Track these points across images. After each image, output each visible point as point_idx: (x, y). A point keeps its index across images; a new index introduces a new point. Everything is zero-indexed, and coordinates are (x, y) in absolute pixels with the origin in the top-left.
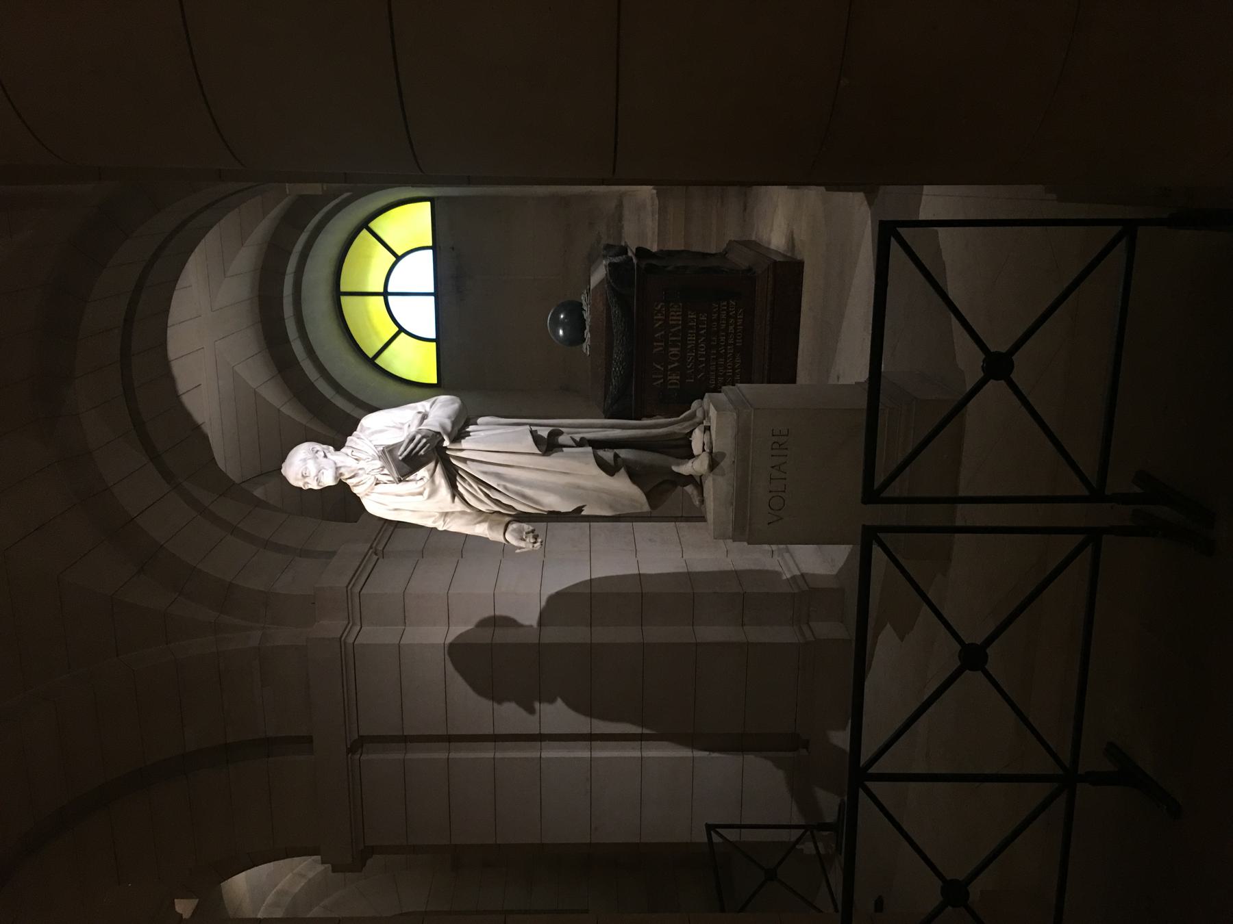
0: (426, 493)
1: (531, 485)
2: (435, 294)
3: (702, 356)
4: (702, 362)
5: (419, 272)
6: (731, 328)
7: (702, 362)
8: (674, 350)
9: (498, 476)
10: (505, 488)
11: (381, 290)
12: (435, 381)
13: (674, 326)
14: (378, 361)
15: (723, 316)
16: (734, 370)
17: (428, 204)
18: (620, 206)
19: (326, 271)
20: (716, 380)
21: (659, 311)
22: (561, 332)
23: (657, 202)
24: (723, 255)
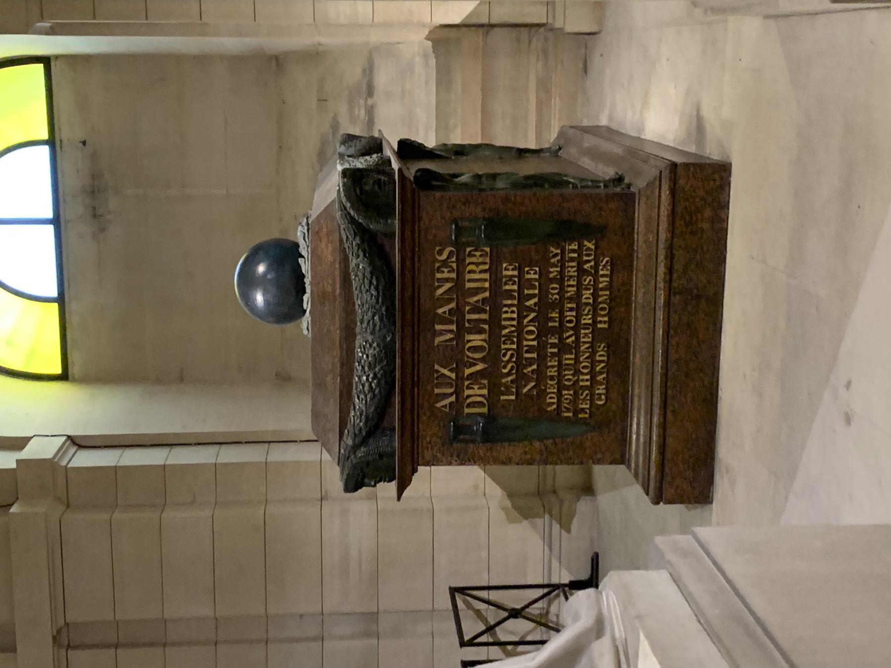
3: (530, 349)
4: (530, 362)
6: (587, 294)
7: (530, 362)
8: (476, 340)
12: (58, 370)
13: (477, 291)
15: (573, 272)
16: (593, 374)
18: (369, 71)
21: (445, 263)
23: (433, 62)
24: (555, 152)
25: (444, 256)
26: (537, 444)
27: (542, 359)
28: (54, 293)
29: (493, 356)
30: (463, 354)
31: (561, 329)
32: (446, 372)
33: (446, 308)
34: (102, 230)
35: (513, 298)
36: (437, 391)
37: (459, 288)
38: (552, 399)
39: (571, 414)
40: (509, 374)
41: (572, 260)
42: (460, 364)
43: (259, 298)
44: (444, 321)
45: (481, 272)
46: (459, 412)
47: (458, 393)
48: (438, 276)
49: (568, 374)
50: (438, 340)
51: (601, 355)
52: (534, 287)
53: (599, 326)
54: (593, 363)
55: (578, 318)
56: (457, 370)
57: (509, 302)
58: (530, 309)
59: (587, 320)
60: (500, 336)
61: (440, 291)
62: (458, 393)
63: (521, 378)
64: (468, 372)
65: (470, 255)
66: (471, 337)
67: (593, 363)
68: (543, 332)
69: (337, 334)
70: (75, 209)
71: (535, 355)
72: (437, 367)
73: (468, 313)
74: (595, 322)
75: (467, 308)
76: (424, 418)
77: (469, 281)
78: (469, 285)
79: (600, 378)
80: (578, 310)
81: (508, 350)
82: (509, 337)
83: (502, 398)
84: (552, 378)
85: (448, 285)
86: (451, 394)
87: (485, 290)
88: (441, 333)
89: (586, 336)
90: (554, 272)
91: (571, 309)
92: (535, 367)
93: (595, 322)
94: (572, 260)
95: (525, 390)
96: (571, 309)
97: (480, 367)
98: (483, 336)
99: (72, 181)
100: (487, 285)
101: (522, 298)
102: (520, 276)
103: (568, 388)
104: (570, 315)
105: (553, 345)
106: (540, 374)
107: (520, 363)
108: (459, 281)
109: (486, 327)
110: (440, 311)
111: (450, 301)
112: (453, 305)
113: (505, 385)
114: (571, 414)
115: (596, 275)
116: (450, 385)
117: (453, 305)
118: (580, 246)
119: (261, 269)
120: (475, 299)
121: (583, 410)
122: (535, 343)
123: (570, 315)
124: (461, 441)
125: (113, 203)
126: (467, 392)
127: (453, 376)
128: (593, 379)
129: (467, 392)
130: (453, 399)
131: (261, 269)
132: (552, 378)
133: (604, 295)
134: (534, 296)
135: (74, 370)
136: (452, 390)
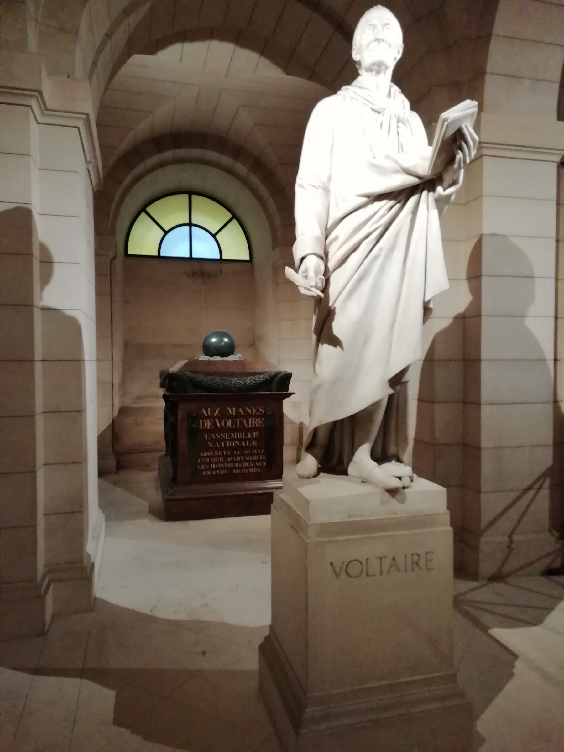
2: (191, 258)
3: (225, 444)
5: (205, 249)
6: (246, 464)
7: (220, 445)
8: (229, 423)
9: (392, 249)
10: (376, 258)
11: (188, 222)
12: (130, 252)
14: (143, 215)
15: (256, 458)
16: (215, 469)
17: (247, 258)
19: (209, 186)
20: (207, 457)
21: (258, 411)
22: (214, 340)
25: (261, 410)
27: (221, 449)
29: (223, 430)
31: (232, 455)
32: (217, 412)
33: (241, 412)
35: (245, 436)
36: (209, 409)
37: (248, 416)
39: (199, 461)
40: (216, 437)
41: (259, 458)
42: (220, 418)
44: (237, 410)
45: (255, 424)
47: (208, 417)
48: (254, 408)
50: (229, 409)
51: (223, 472)
52: (249, 444)
53: (234, 470)
54: (220, 469)
55: (238, 462)
56: (217, 417)
58: (241, 443)
59: (237, 465)
61: (248, 409)
62: (208, 417)
63: (214, 441)
64: (217, 421)
65: (261, 420)
66: (230, 421)
67: (220, 469)
68: (232, 449)
69: (231, 370)
70: (196, 266)
72: (219, 409)
73: (240, 420)
74: (236, 468)
77: (252, 420)
78: (250, 419)
79: (214, 473)
80: (241, 462)
81: (225, 435)
82: (230, 436)
83: (206, 435)
84: (214, 453)
85: (250, 412)
87: (248, 425)
89: (230, 465)
90: (255, 451)
91: (241, 459)
93: (236, 468)
94: (259, 458)
95: (209, 443)
96: (241, 459)
97: (219, 425)
98: (230, 426)
99: (207, 267)
100: (250, 426)
101: (245, 440)
102: (254, 439)
103: (210, 460)
104: (239, 459)
105: (227, 453)
106: (215, 449)
107: (220, 441)
108: (251, 416)
110: (240, 409)
112: (242, 414)
113: (212, 435)
114: (199, 461)
115: (253, 467)
117: (242, 414)
118: (264, 461)
119: (226, 340)
121: (201, 467)
122: (228, 446)
123: (239, 459)
126: (208, 421)
128: (213, 469)
129: (208, 421)
130: (206, 415)
131: (226, 340)
132: (214, 453)
133: (246, 471)
134: (246, 443)
136: (209, 415)
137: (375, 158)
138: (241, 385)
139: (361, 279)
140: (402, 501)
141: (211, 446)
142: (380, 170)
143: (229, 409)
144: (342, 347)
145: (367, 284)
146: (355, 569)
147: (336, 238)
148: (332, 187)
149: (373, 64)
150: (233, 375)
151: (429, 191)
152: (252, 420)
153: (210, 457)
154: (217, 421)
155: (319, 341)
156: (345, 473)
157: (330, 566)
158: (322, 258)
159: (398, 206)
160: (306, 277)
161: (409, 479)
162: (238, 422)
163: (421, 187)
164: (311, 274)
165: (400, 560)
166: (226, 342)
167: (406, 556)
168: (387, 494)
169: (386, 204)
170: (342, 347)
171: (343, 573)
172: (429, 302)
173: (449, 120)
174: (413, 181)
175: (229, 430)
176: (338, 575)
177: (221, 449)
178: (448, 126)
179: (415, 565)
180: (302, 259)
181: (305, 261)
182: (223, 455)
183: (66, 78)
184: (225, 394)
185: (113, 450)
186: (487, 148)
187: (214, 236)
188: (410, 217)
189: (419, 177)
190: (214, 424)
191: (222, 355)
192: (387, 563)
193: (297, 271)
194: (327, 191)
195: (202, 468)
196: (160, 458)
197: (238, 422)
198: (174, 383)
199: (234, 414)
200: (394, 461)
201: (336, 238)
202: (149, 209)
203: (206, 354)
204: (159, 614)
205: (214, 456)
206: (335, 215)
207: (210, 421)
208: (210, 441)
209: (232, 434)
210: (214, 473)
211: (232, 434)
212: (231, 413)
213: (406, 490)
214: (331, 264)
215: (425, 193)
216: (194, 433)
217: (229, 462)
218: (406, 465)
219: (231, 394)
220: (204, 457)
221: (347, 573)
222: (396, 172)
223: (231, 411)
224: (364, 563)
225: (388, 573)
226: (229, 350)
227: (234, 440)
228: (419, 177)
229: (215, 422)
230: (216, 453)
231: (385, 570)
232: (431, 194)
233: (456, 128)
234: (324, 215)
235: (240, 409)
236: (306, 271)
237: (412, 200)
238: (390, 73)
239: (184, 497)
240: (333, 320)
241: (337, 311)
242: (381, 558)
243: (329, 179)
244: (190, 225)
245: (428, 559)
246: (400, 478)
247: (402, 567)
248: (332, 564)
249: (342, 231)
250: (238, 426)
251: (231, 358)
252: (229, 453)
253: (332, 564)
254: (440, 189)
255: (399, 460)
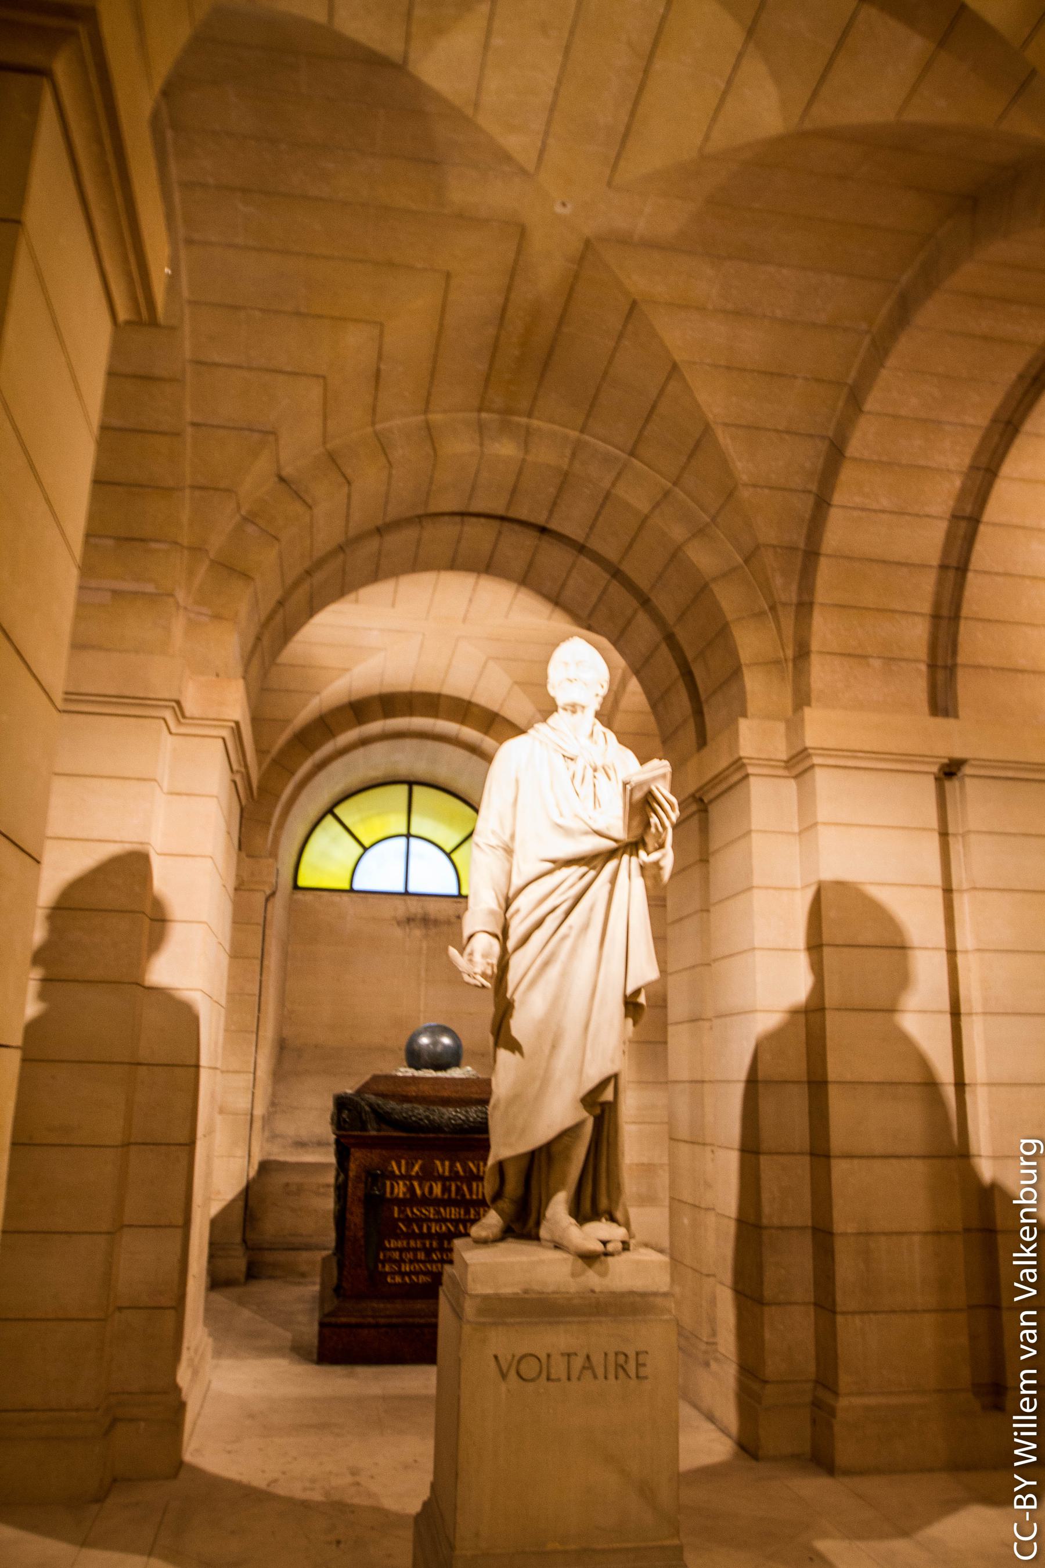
0: (560, 821)
1: (564, 974)
3: (429, 1228)
7: (420, 1228)
8: (437, 1190)
9: (586, 927)
10: (565, 937)
11: (404, 831)
12: (301, 883)
19: (442, 773)
20: (396, 1249)
26: (360, 1234)
27: (422, 1236)
28: (357, 886)
29: (426, 1201)
30: (428, 1180)
32: (416, 1168)
34: (399, 923)
36: (403, 1162)
38: (393, 1244)
40: (413, 1213)
43: (424, 1040)
44: (452, 1167)
46: (388, 1178)
47: (402, 1177)
49: (410, 1255)
50: (438, 1163)
51: (422, 1279)
54: (417, 1273)
56: (417, 1177)
57: (462, 1212)
58: (456, 1227)
60: (439, 1206)
61: (471, 1165)
62: (402, 1177)
63: (408, 1221)
64: (416, 1184)
66: (440, 1185)
67: (417, 1273)
69: (445, 1094)
70: (414, 907)
71: (425, 1230)
72: (420, 1162)
73: (457, 1186)
75: (459, 1184)
76: (384, 1152)
77: (478, 1186)
79: (407, 1279)
82: (438, 1213)
83: (396, 1209)
84: (408, 1244)
85: (475, 1170)
86: (400, 1171)
88: (443, 1165)
92: (417, 1231)
97: (418, 1192)
99: (433, 908)
100: (474, 1197)
103: (401, 1256)
105: (431, 1244)
107: (419, 1221)
109: (446, 1196)
110: (458, 1165)
111: (464, 1171)
112: (462, 1173)
113: (405, 1211)
116: (407, 1170)
119: (446, 1040)
120: (465, 1188)
121: (384, 1266)
122: (433, 1231)
124: (367, 1179)
125: (418, 933)
127: (413, 1173)
129: (401, 1183)
130: (397, 1172)
132: (408, 1244)
135: (299, 896)
137: (561, 815)
138: (460, 1122)
139: (546, 964)
140: (603, 1274)
141: (404, 1229)
142: (567, 832)
143: (438, 1163)
144: (521, 1053)
145: (553, 972)
146: (529, 1368)
147: (517, 911)
148: (517, 846)
149: (568, 705)
150: (446, 1102)
151: (631, 855)
152: (478, 1186)
153: (401, 1250)
154: (416, 1184)
155: (496, 1045)
156: (537, 1238)
157: (493, 1359)
158: (496, 936)
159: (592, 873)
160: (471, 961)
161: (620, 1246)
162: (453, 1188)
163: (621, 851)
164: (478, 958)
165: (597, 1359)
166: (445, 1047)
167: (606, 1354)
168: (580, 1261)
169: (576, 871)
170: (521, 1053)
171: (513, 1372)
172: (637, 992)
173: (633, 784)
174: (612, 845)
175: (437, 1202)
176: (504, 1376)
177: (422, 1236)
178: (632, 790)
179: (621, 1371)
180: (471, 937)
181: (474, 940)
182: (424, 1248)
183: (214, 678)
184: (431, 1135)
185: (244, 1241)
186: (816, 755)
187: (448, 855)
188: (608, 886)
189: (616, 841)
190: (411, 1189)
191: (437, 1068)
192: (578, 1363)
193: (461, 951)
194: (509, 851)
195: (387, 1269)
196: (325, 1260)
197: (453, 1188)
198: (345, 1115)
199: (447, 1174)
200: (604, 1220)
201: (517, 911)
202: (338, 811)
203: (411, 1065)
204: (280, 1490)
205: (408, 1249)
206: (517, 882)
207: (405, 1184)
208: (402, 1221)
209: (442, 1210)
210: (407, 1279)
211: (442, 1210)
212: (440, 1170)
213: (610, 1259)
214: (511, 944)
215: (626, 857)
216: (376, 1204)
217: (432, 1261)
218: (619, 1225)
219: (442, 1136)
220: (390, 1249)
221: (518, 1373)
222: (586, 833)
223: (442, 1167)
224: (544, 1360)
225: (579, 1379)
226: (452, 1058)
227: (445, 1220)
228: (616, 841)
229: (412, 1185)
230: (412, 1244)
231: (575, 1373)
232: (634, 859)
233: (645, 789)
234: (503, 881)
235: (458, 1165)
236: (471, 954)
237: (611, 865)
238: (590, 713)
239: (353, 1320)
240: (511, 1016)
241: (516, 1005)
242: (569, 1355)
243: (513, 837)
244: (408, 836)
245: (640, 1362)
246: (605, 1243)
247: (600, 1371)
248: (496, 1357)
249: (522, 903)
250: (453, 1195)
251: (455, 1073)
252: (435, 1244)
253: (496, 1357)
254: (642, 853)
255: (612, 1219)
